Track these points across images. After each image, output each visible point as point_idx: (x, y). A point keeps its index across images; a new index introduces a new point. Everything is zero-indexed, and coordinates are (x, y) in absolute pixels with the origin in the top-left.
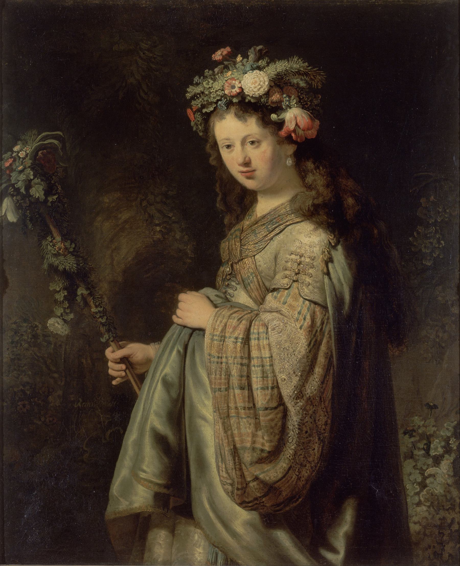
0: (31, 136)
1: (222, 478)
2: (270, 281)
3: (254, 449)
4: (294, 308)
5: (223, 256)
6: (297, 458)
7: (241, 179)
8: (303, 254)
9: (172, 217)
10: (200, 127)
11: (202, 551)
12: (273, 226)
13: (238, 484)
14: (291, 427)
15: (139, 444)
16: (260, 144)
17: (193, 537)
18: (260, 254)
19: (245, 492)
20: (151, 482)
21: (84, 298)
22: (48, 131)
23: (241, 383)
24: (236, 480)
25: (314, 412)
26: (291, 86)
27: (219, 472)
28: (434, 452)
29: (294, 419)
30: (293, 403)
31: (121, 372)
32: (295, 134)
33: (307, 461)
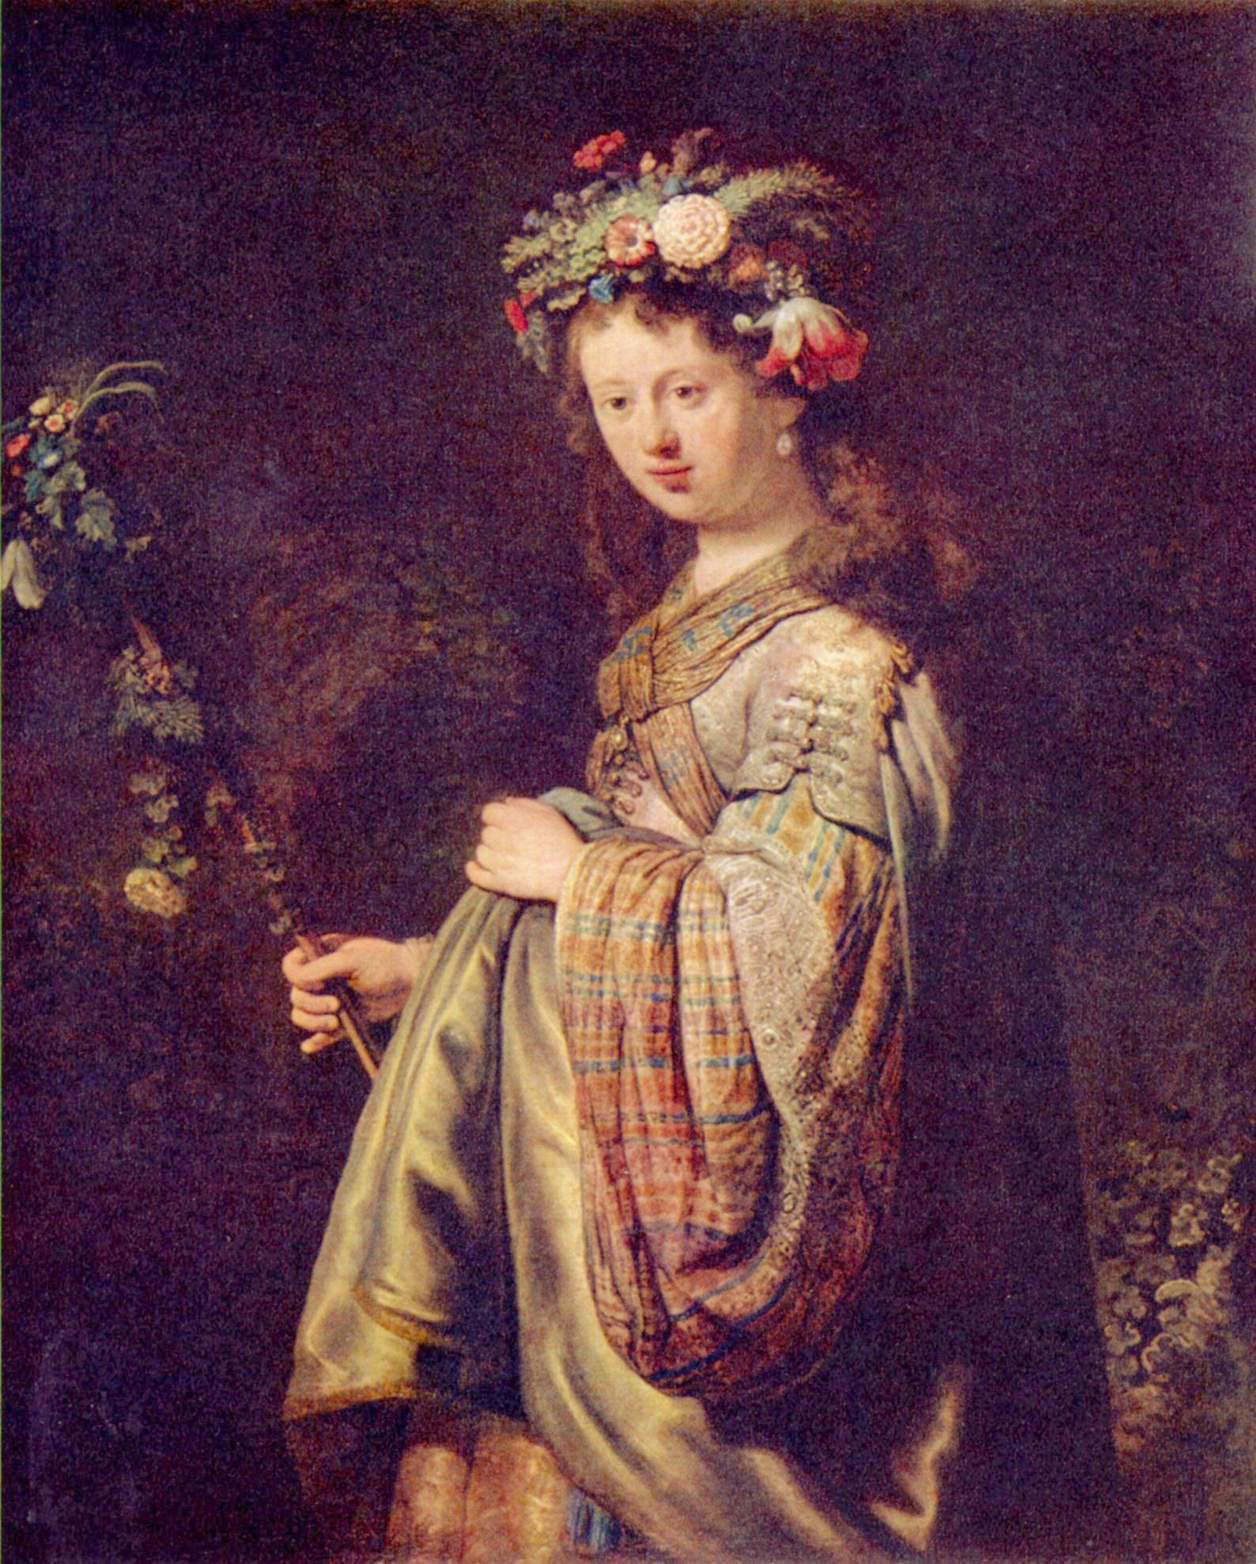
1: (602, 1308)
7: (656, 493)
11: (549, 1506)
13: (646, 1324)
14: (789, 1169)
16: (704, 397)
18: (704, 695)
20: (406, 1316)
24: (640, 1312)
27: (594, 1291)
29: (798, 1149)
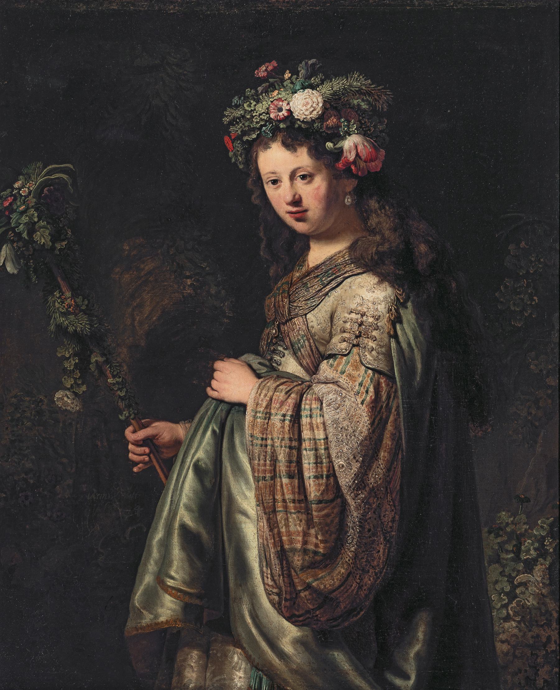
0: (35, 170)
2: (325, 345)
3: (305, 551)
4: (354, 379)
5: (268, 314)
6: (358, 562)
7: (290, 220)
8: (365, 312)
9: (206, 268)
10: (240, 158)
11: (242, 676)
12: (329, 279)
13: (286, 594)
14: (350, 524)
15: (166, 544)
16: (313, 179)
17: (232, 658)
18: (312, 312)
19: (294, 603)
21: (98, 366)
22: (56, 164)
23: (290, 470)
24: (284, 589)
25: (379, 506)
26: (349, 108)
27: (263, 579)
28: (526, 555)
29: (354, 515)
30: (352, 494)
31: (144, 457)
32: (355, 167)
33: (370, 565)
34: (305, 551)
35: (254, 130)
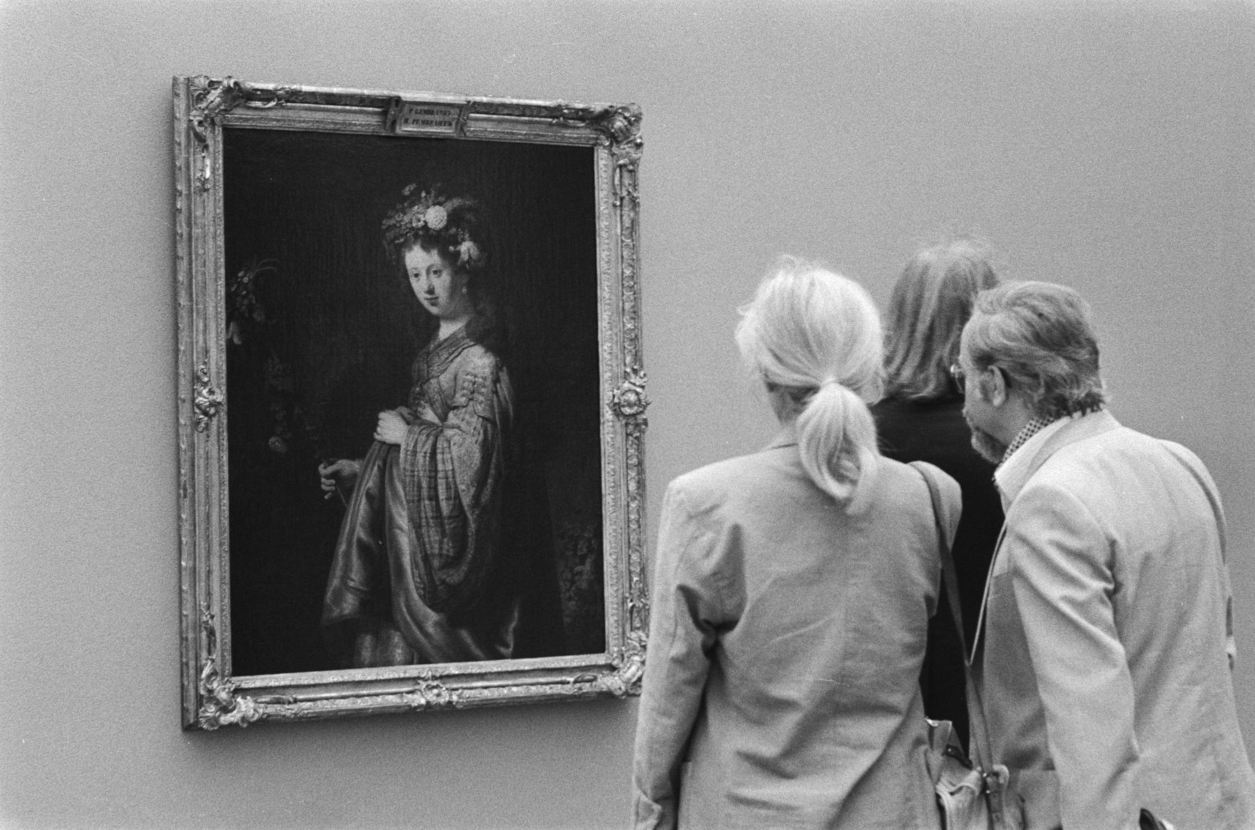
7: (426, 304)
15: (347, 555)
34: (441, 555)
35: (402, 235)
